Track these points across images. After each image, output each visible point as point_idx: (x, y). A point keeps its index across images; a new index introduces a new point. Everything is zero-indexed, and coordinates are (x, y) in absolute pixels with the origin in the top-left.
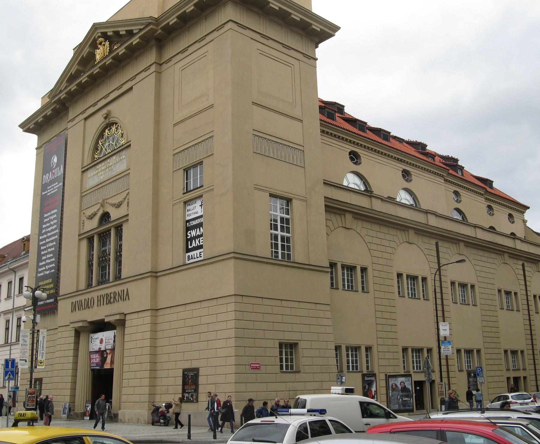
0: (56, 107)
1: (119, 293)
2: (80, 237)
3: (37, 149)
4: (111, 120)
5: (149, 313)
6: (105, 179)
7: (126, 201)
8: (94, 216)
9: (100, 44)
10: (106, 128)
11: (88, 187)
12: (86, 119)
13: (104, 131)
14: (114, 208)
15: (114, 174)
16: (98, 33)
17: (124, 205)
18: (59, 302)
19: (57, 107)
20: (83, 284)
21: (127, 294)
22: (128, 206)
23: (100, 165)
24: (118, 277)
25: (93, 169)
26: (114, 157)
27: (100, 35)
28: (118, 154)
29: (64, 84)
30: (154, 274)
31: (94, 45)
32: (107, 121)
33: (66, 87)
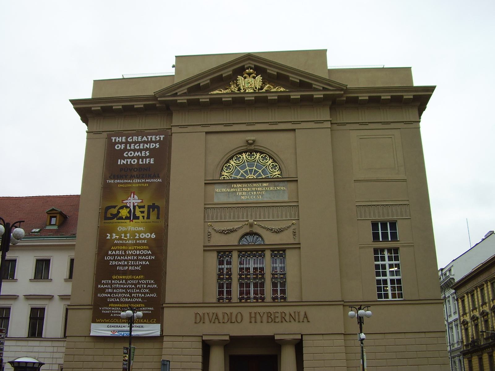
0: (155, 105)
1: (290, 315)
2: (206, 249)
3: (87, 132)
4: (256, 147)
5: (342, 337)
6: (250, 201)
7: (291, 230)
8: (232, 232)
9: (249, 74)
10: (245, 152)
11: (216, 201)
12: (207, 133)
13: (241, 153)
14: (269, 233)
15: (266, 200)
16: (253, 64)
17: (289, 233)
18: (165, 309)
19: (157, 105)
20: (213, 297)
21: (306, 316)
22: (294, 235)
23: (239, 185)
24: (281, 296)
25: (225, 185)
26: (265, 184)
27: (253, 66)
28: (273, 183)
29: (184, 90)
30: (343, 303)
31: (241, 71)
32: (252, 147)
33: (184, 94)
